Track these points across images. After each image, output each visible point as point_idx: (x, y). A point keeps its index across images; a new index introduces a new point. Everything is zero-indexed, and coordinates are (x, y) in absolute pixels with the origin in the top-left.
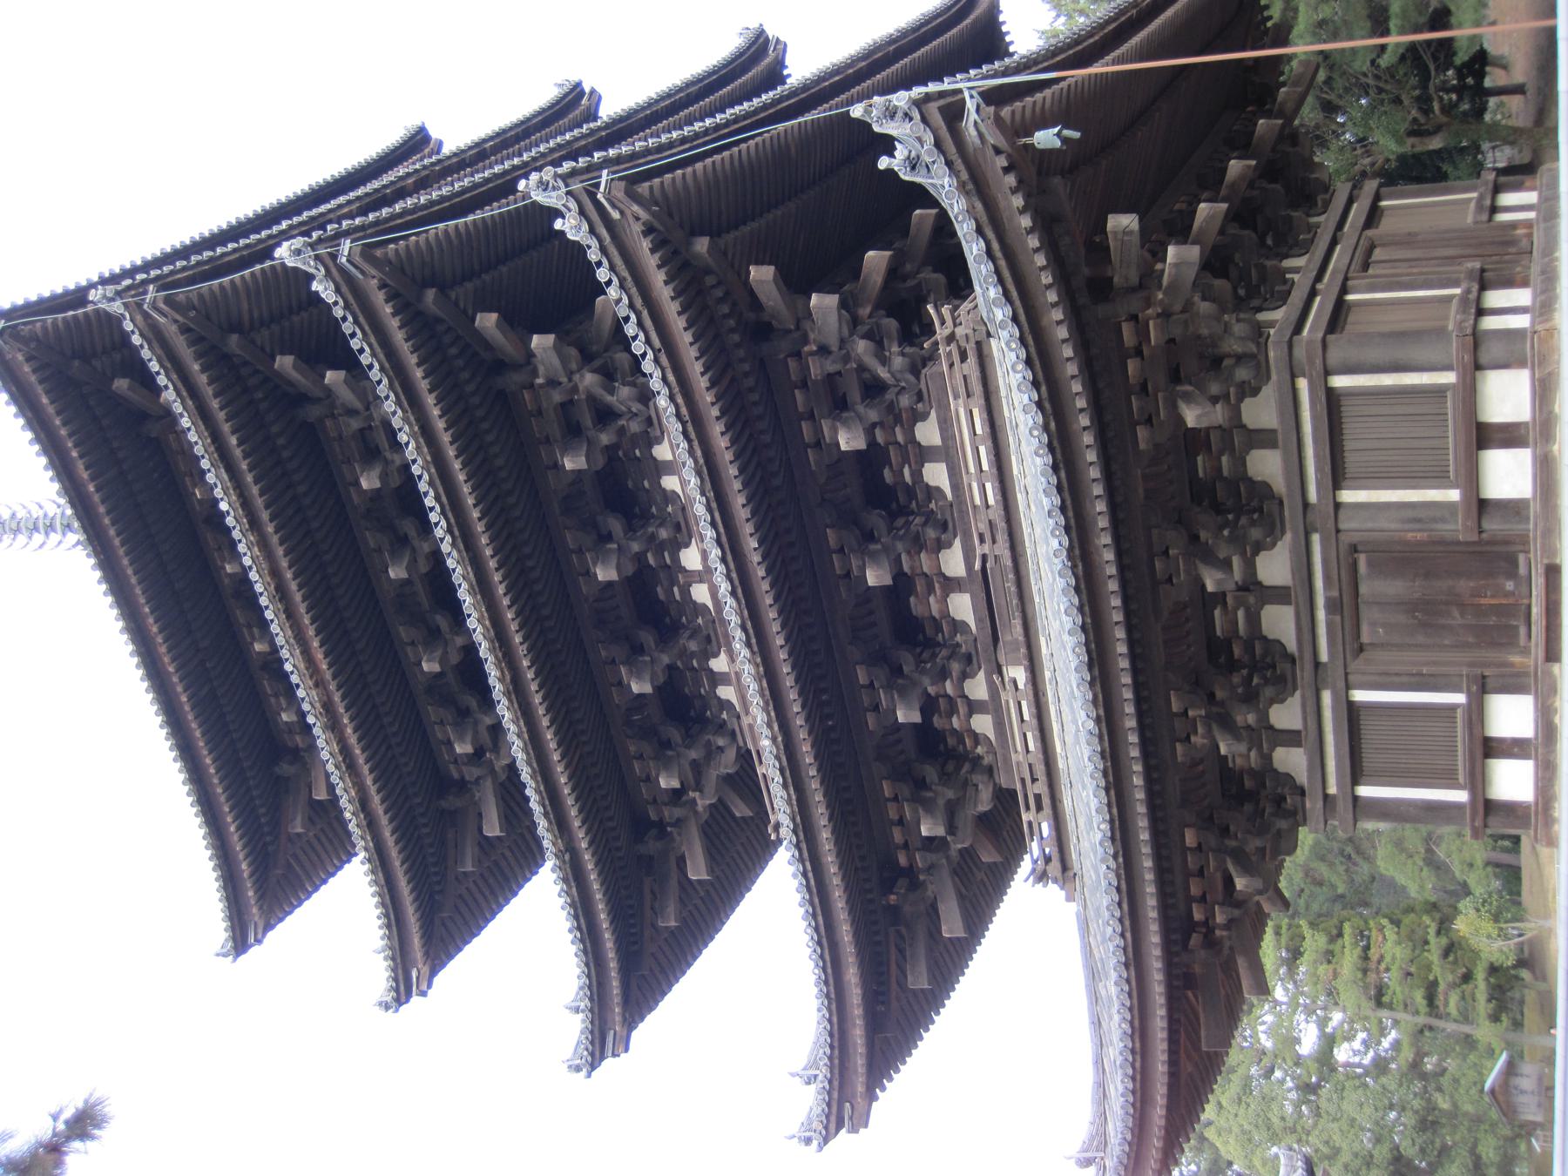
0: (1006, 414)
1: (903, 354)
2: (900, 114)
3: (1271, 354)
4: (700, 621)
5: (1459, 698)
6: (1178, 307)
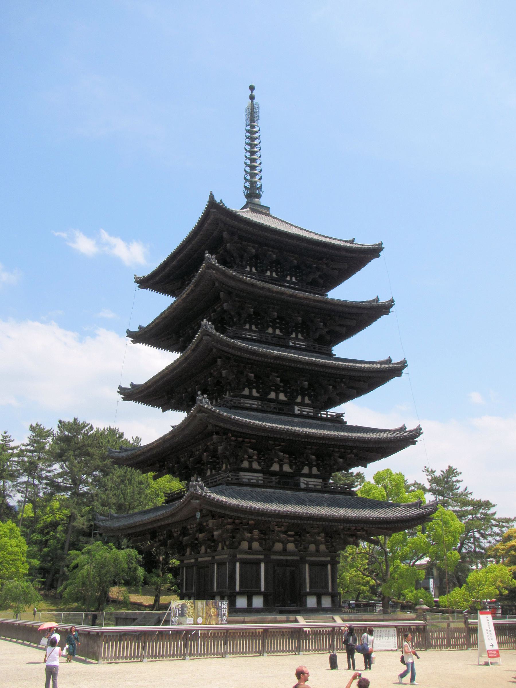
5: (263, 589)
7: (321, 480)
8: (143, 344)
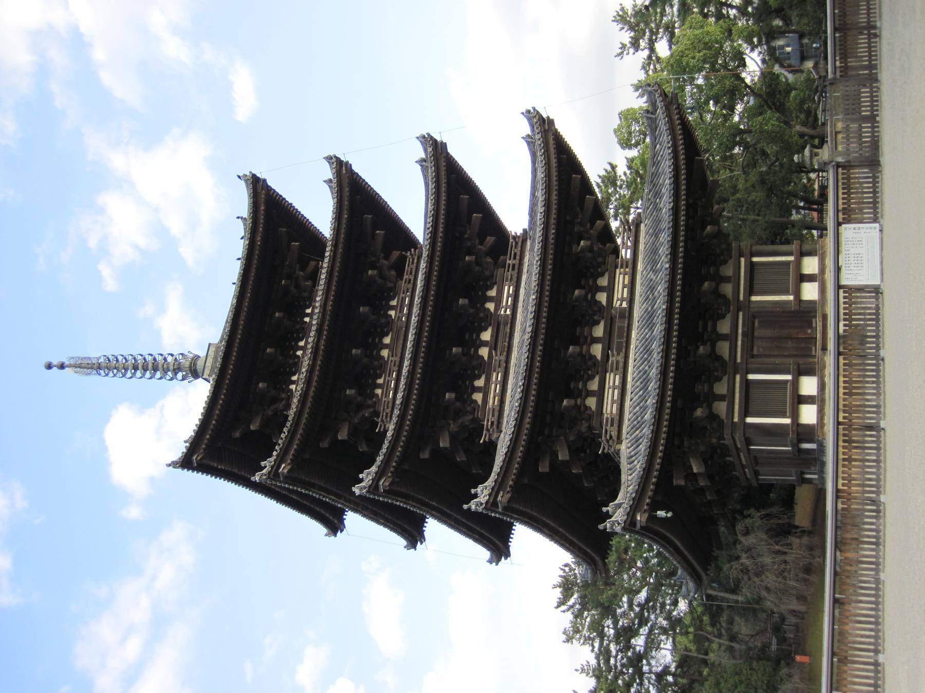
5: (789, 377)
7: (618, 271)
8: (425, 527)
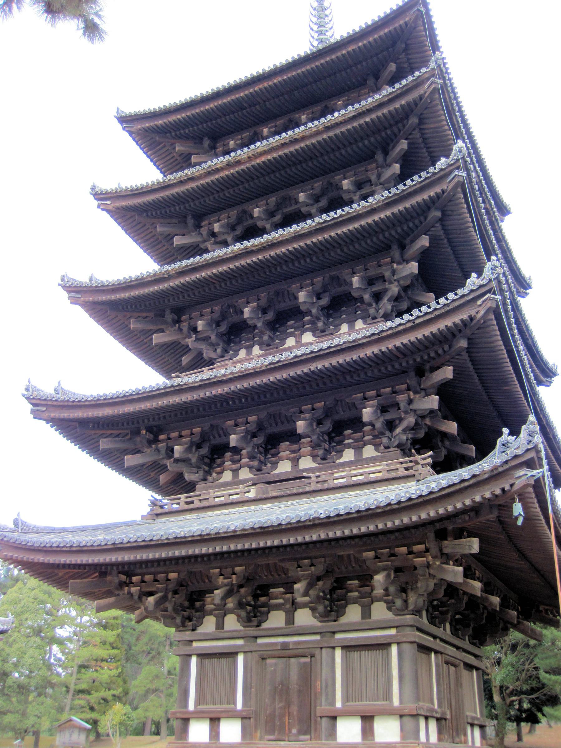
0: (380, 489)
1: (407, 440)
2: (530, 438)
3: (408, 617)
4: (277, 341)
5: (239, 706)
6: (432, 572)
